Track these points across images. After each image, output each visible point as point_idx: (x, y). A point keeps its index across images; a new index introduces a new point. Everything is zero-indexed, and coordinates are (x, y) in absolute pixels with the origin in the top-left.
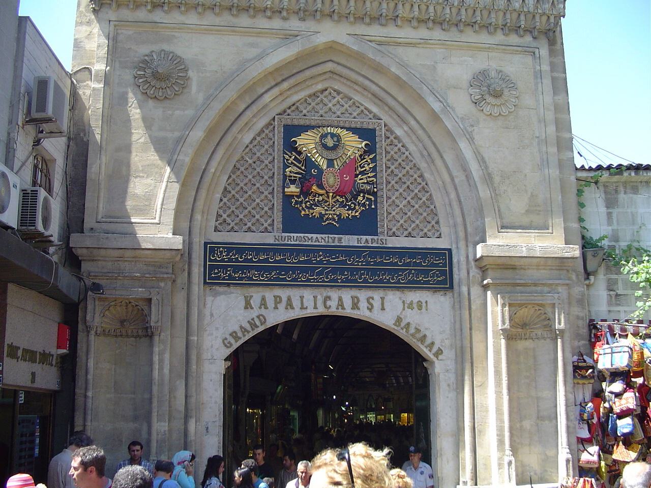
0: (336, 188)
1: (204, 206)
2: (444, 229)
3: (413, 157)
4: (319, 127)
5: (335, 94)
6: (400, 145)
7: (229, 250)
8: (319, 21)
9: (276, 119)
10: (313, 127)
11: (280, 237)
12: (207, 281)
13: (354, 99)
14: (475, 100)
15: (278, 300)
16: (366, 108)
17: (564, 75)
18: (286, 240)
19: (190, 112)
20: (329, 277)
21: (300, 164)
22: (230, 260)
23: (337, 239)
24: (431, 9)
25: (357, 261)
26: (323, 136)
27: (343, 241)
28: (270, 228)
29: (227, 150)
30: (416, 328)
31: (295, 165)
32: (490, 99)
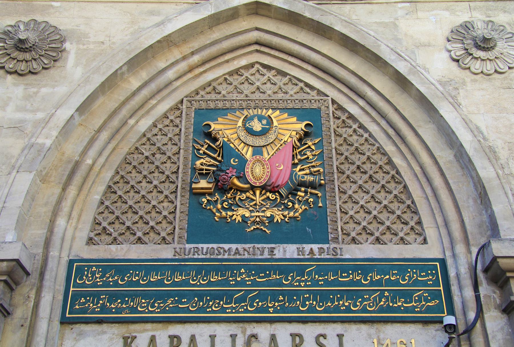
0: (265, 179)
2: (431, 233)
3: (376, 140)
5: (264, 71)
6: (355, 126)
7: (105, 270)
10: (232, 110)
11: (182, 250)
12: (67, 315)
13: (290, 75)
14: (456, 56)
16: (307, 85)
18: (192, 253)
19: (62, 90)
20: (255, 304)
21: (215, 154)
25: (300, 281)
26: (246, 119)
27: (276, 252)
28: (169, 238)
29: (112, 137)
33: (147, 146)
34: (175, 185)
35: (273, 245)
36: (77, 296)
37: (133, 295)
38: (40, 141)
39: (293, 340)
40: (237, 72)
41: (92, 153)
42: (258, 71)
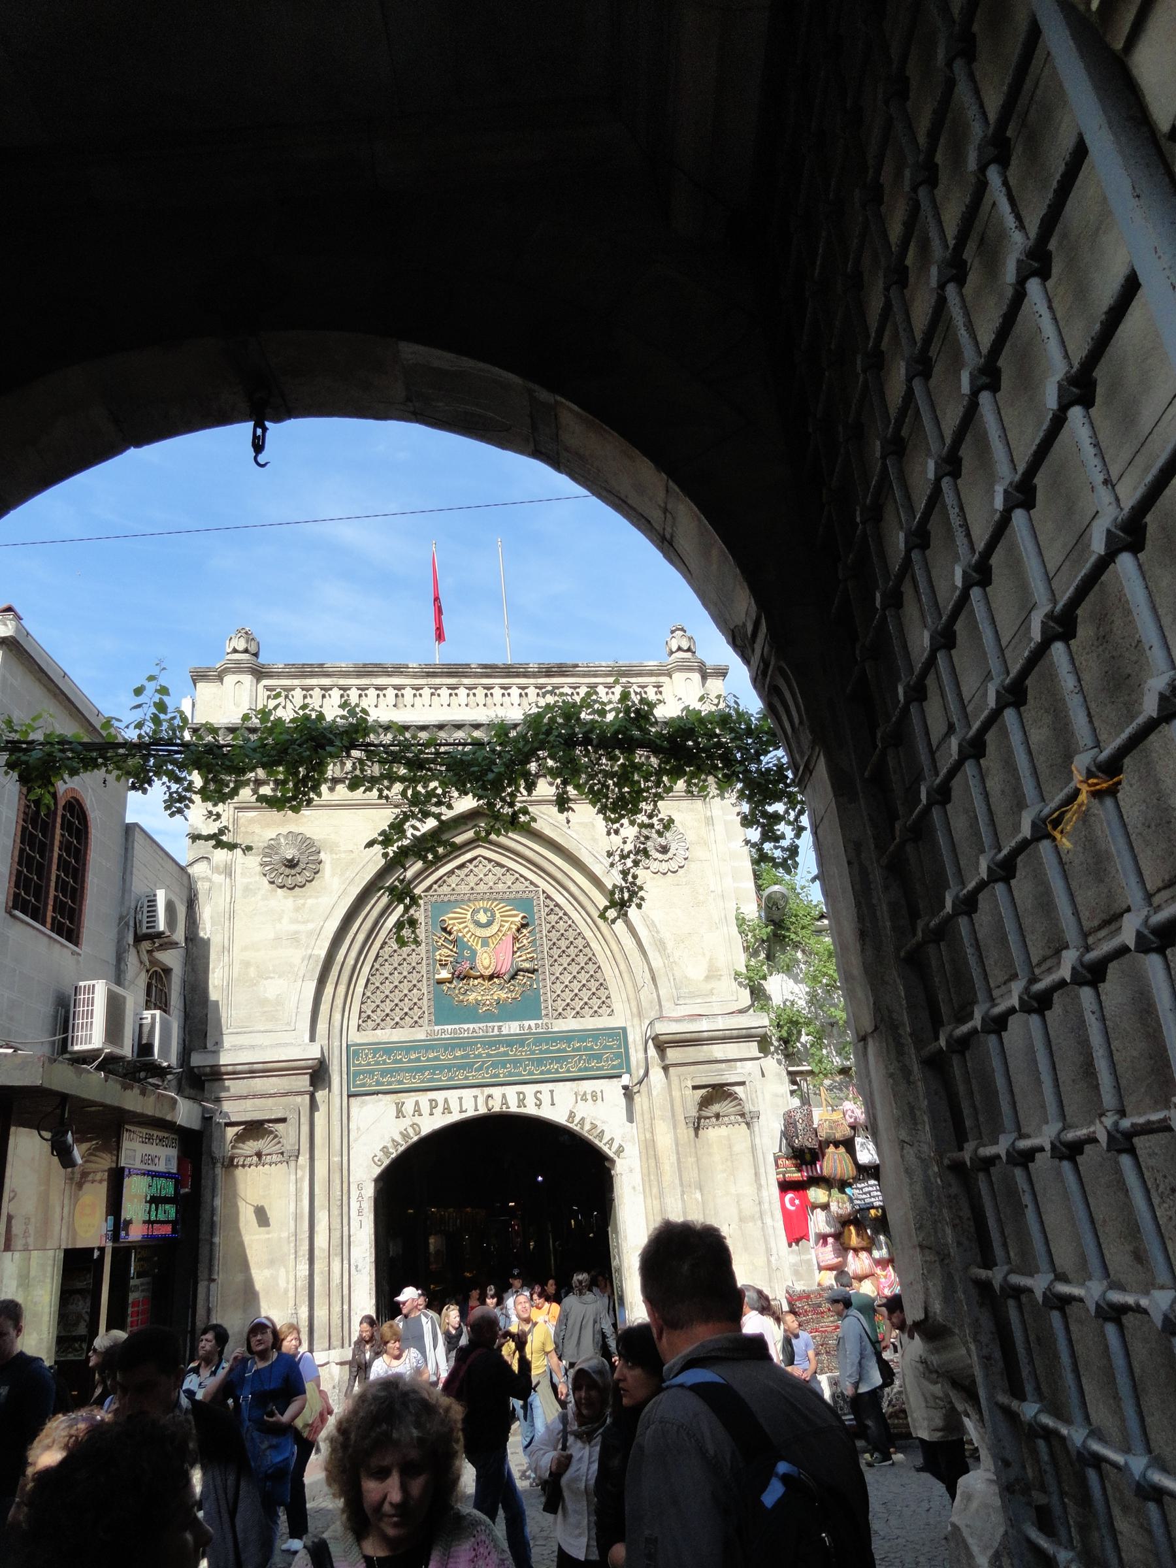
4: (469, 900)
15: (433, 1104)
16: (521, 876)
19: (326, 901)
23: (496, 1028)
25: (521, 1051)
27: (503, 1029)
35: (501, 1024)
36: (357, 1074)
38: (316, 952)
39: (519, 1097)
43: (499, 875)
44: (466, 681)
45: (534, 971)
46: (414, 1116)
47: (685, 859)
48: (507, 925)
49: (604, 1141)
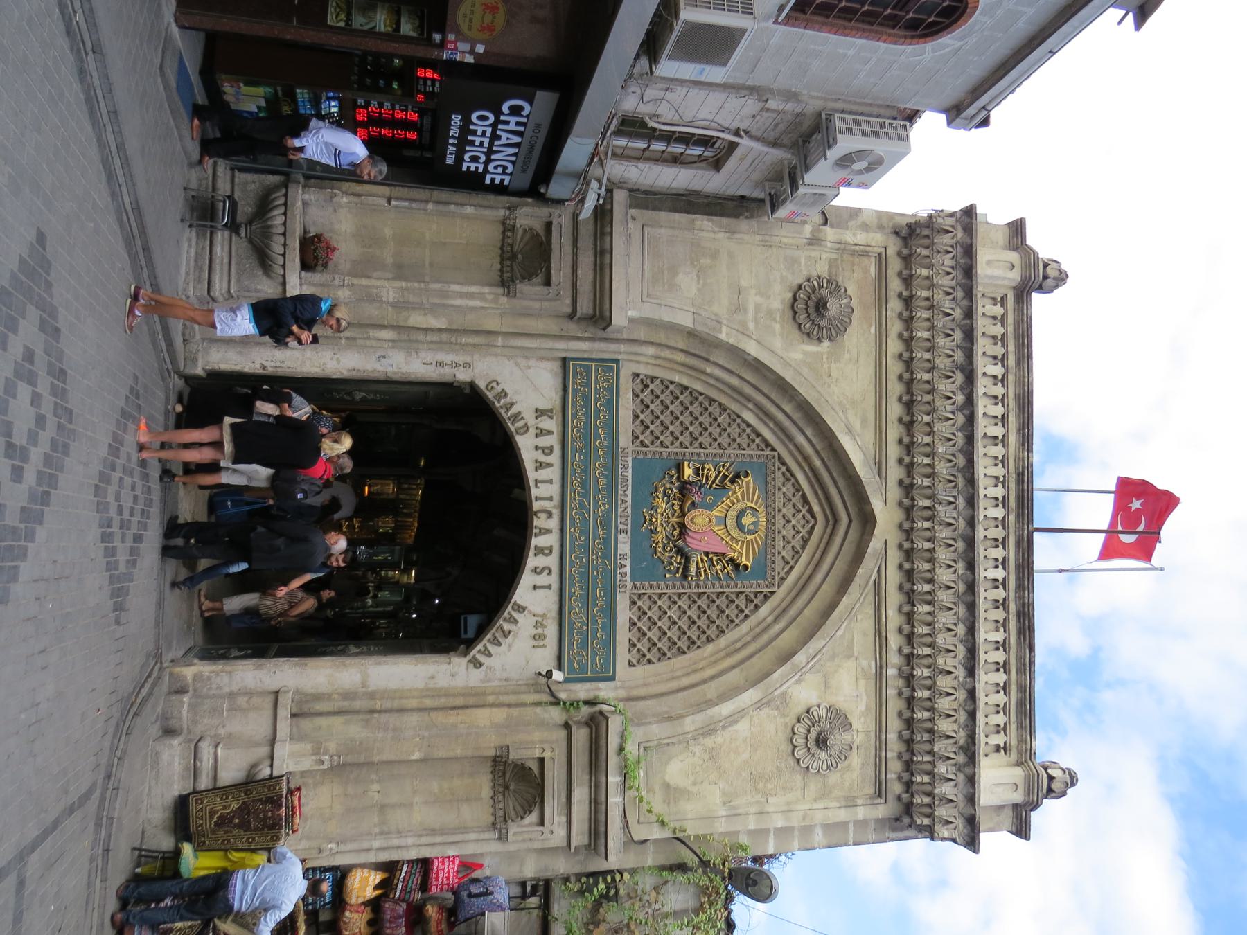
1: (665, 359)
2: (639, 671)
3: (732, 630)
4: (766, 507)
5: (808, 527)
8: (900, 504)
9: (773, 453)
15: (548, 451)
16: (792, 568)
17: (851, 843)
19: (778, 344)
22: (597, 392)
23: (623, 527)
24: (927, 651)
27: (623, 535)
30: (510, 632)
31: (717, 477)
32: (813, 736)
33: (728, 420)
34: (688, 445)
36: (588, 369)
37: (587, 415)
38: (724, 329)
39: (546, 548)
40: (805, 500)
41: (718, 372)
42: (808, 522)
43: (794, 543)
44: (1012, 518)
45: (685, 576)
46: (537, 428)
47: (808, 768)
48: (738, 547)
49: (490, 647)
